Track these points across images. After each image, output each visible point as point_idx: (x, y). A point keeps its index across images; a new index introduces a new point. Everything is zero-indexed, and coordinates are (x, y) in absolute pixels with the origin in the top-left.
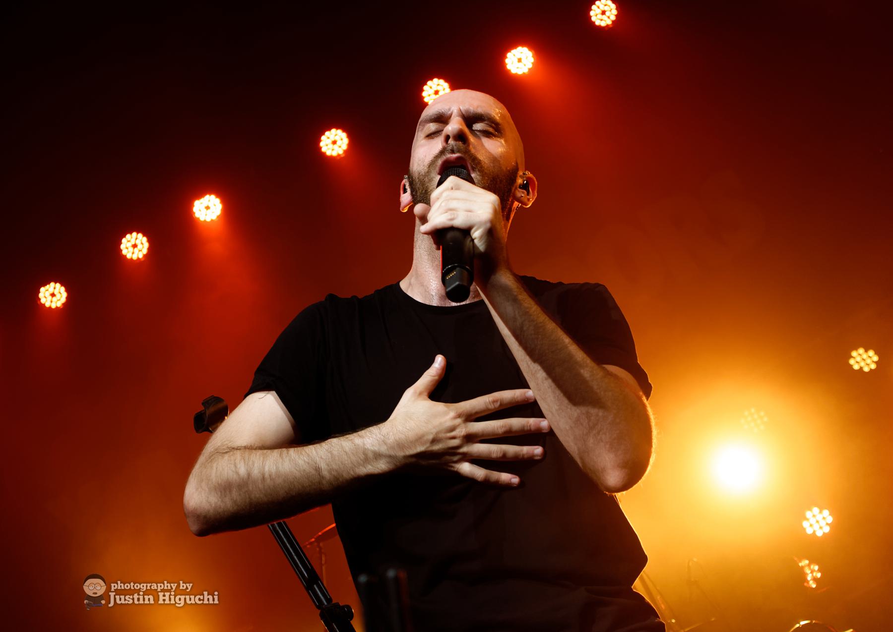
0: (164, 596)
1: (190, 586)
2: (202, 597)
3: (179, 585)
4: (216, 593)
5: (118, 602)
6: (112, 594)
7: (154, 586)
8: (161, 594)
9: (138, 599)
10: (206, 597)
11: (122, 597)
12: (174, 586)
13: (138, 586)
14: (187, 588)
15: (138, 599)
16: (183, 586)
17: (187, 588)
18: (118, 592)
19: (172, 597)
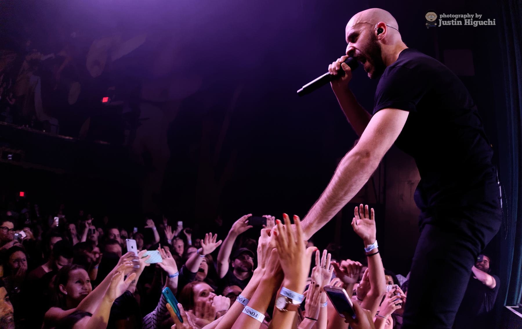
1: (481, 16)
5: (443, 24)
6: (440, 20)
7: (462, 16)
8: (466, 20)
9: (454, 23)
11: (446, 22)
12: (472, 16)
13: (453, 16)
15: (454, 23)
16: (477, 16)
18: (444, 19)
19: (472, 22)
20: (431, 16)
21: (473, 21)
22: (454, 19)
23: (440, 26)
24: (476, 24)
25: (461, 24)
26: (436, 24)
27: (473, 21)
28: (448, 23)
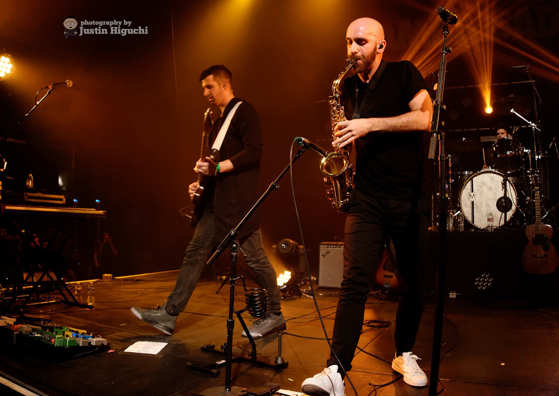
0: (114, 29)
1: (130, 23)
3: (123, 23)
4: (146, 27)
5: (85, 33)
6: (81, 28)
7: (108, 23)
8: (112, 28)
9: (98, 31)
10: (140, 30)
11: (88, 30)
12: (120, 23)
13: (97, 23)
14: (128, 24)
15: (98, 31)
16: (126, 23)
18: (85, 27)
19: (119, 30)
20: (70, 24)
21: (121, 29)
22: (97, 26)
23: (81, 34)
24: (124, 32)
25: (106, 33)
26: (76, 33)
27: (121, 29)
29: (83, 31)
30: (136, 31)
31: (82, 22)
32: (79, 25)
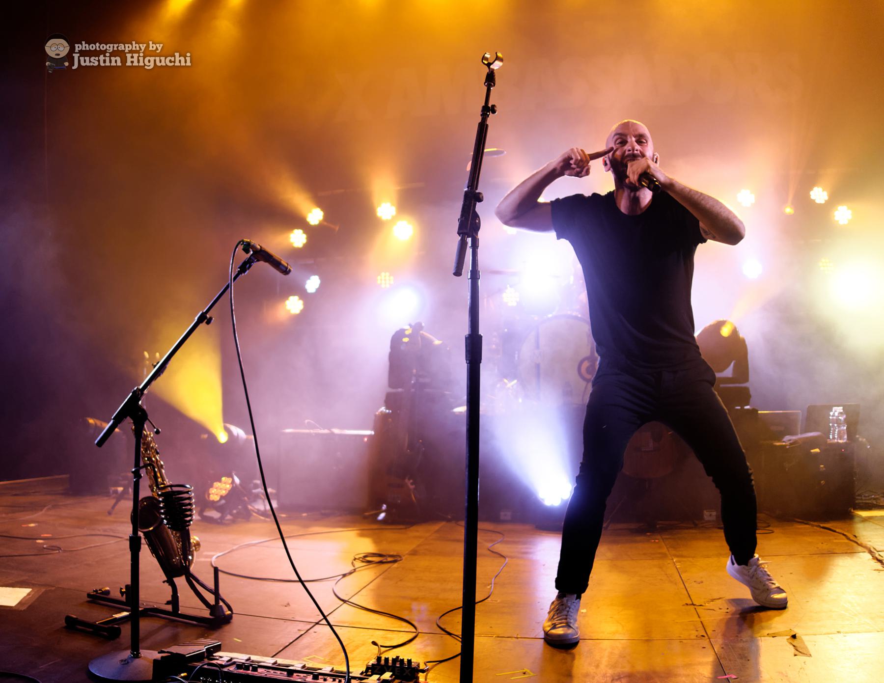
0: (132, 57)
2: (173, 59)
3: (148, 46)
5: (83, 64)
6: (76, 56)
7: (122, 47)
8: (128, 56)
9: (105, 61)
10: (177, 59)
11: (87, 59)
12: (143, 47)
13: (104, 47)
14: (157, 49)
15: (105, 61)
17: (157, 49)
18: (83, 53)
19: (141, 59)
20: (56, 48)
21: (144, 57)
22: (104, 53)
23: (75, 67)
25: (119, 64)
26: (67, 64)
27: (144, 57)
28: (93, 61)
29: (79, 61)
30: (170, 61)
31: (76, 45)
32: (72, 50)
